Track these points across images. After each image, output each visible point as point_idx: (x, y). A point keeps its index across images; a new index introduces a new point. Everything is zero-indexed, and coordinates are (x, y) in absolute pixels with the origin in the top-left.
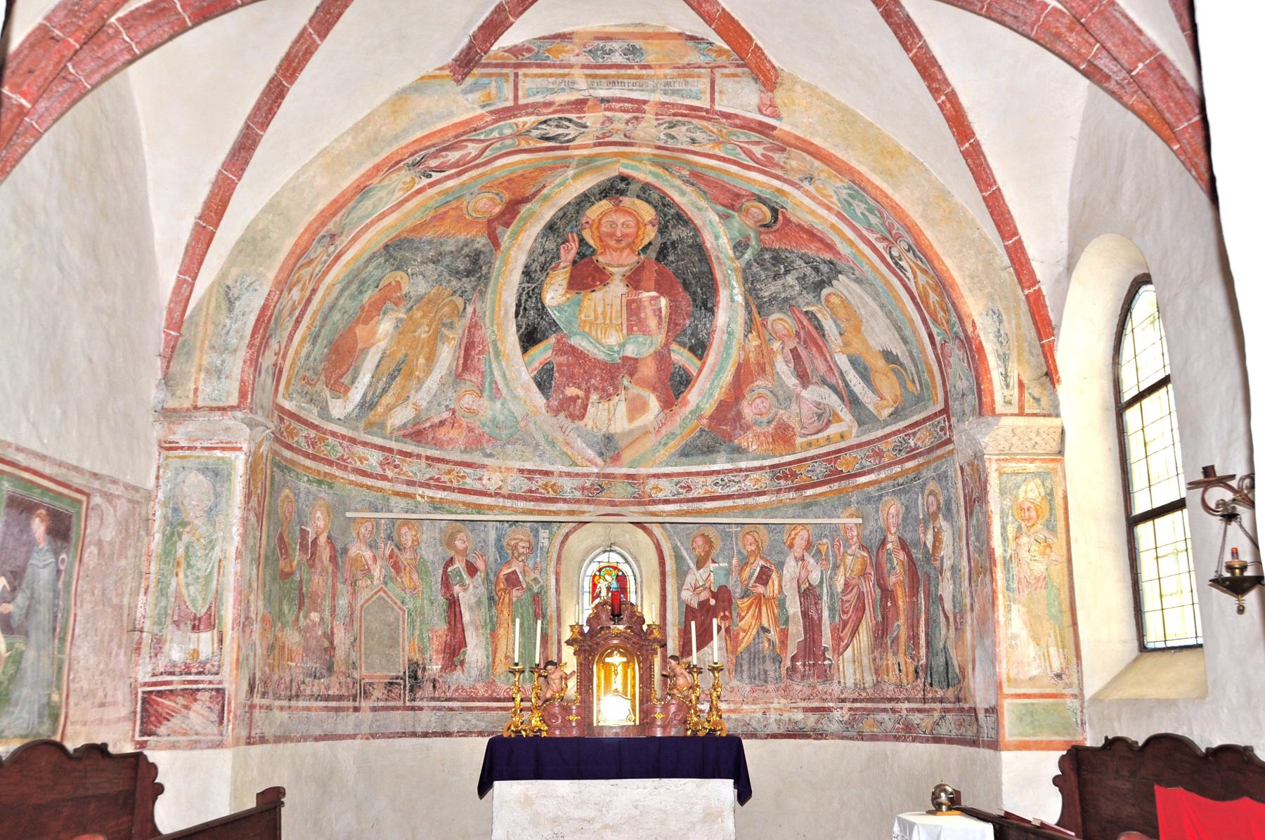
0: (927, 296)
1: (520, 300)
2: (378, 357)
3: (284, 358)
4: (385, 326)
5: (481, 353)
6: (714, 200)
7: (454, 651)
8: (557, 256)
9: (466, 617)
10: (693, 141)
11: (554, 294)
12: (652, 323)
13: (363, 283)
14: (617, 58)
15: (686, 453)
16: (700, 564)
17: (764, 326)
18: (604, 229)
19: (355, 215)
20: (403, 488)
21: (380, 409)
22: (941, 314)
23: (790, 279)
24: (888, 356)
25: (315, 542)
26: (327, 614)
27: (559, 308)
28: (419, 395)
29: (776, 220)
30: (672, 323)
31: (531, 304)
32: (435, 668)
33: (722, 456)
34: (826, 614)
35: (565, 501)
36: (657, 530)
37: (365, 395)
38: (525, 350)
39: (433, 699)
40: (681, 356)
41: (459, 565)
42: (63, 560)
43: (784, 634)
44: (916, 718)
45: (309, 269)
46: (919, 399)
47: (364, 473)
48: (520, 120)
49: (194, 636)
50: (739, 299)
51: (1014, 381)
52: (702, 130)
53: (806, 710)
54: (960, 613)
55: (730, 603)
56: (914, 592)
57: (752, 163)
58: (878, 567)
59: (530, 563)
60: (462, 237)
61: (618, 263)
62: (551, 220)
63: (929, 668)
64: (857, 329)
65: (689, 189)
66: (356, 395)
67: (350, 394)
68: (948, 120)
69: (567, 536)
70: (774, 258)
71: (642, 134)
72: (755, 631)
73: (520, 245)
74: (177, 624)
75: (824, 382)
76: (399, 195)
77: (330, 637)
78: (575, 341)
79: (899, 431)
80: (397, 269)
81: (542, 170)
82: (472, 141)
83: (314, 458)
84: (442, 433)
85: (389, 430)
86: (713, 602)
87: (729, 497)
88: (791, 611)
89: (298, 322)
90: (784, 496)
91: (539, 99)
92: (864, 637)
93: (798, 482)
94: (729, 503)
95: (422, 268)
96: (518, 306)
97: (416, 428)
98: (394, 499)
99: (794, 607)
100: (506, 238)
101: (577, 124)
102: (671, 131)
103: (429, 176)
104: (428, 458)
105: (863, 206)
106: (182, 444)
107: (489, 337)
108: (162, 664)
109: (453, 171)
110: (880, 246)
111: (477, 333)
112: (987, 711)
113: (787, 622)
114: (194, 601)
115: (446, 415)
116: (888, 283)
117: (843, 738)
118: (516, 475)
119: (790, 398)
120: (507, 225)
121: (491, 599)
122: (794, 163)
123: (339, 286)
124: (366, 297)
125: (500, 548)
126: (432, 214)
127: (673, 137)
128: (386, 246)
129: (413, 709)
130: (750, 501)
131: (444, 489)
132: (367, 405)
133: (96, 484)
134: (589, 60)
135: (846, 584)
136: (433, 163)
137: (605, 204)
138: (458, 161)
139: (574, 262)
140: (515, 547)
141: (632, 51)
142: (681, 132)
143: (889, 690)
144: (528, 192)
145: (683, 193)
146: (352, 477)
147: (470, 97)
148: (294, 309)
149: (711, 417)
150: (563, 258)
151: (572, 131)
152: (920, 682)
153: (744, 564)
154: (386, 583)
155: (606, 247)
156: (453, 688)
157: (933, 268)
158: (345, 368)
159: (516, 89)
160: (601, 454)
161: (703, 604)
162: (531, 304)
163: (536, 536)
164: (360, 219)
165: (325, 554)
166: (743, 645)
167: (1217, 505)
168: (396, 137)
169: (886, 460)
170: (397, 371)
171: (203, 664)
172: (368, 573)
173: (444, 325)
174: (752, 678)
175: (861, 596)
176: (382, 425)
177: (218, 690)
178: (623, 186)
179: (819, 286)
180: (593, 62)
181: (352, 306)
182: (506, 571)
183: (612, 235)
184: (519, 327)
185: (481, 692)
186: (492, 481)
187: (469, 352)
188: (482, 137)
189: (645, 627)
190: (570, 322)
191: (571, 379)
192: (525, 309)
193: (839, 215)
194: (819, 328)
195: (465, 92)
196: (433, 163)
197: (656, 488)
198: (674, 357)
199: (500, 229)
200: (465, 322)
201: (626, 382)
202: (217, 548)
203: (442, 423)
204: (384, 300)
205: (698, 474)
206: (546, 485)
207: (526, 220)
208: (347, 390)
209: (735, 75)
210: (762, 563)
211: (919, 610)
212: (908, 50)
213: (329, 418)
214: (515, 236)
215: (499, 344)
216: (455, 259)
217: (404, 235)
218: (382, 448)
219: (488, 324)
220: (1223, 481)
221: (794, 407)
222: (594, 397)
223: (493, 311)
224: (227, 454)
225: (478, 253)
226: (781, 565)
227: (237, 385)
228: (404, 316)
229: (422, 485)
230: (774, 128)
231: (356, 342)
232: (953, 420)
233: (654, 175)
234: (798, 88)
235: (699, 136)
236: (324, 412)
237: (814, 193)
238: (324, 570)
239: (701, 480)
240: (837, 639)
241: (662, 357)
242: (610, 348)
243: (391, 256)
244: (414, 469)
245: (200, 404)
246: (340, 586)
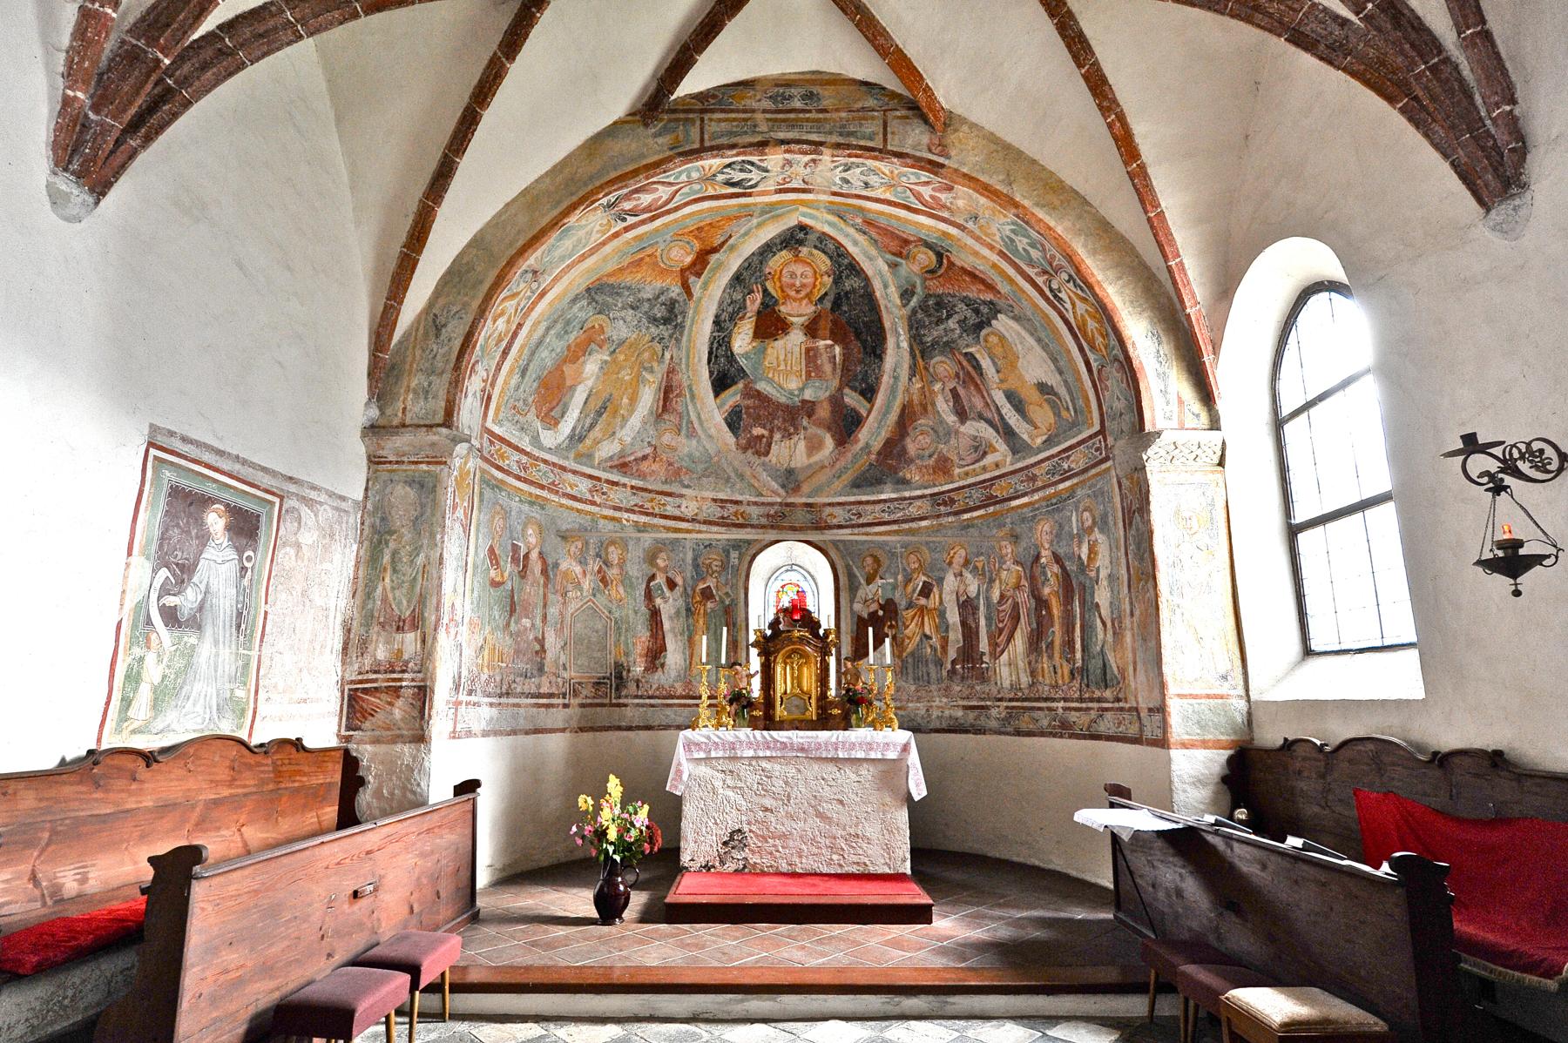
0: (1085, 324)
3: (493, 385)
4: (591, 367)
6: (884, 249)
7: (655, 655)
9: (667, 625)
10: (866, 184)
11: (742, 341)
12: (828, 368)
13: (568, 323)
14: (798, 104)
15: (858, 484)
16: (869, 581)
17: (926, 369)
19: (557, 254)
20: (610, 513)
21: (588, 442)
22: (1099, 340)
23: (952, 323)
24: (1043, 388)
25: (526, 556)
26: (538, 622)
27: (746, 356)
28: (624, 432)
29: (940, 263)
30: (845, 369)
32: (638, 669)
33: (888, 487)
34: (983, 622)
35: (752, 526)
36: (833, 554)
37: (574, 429)
38: (717, 395)
39: (636, 697)
40: (852, 399)
41: (660, 580)
42: (249, 559)
43: (945, 641)
44: (1073, 717)
45: (514, 302)
46: (1074, 425)
47: (574, 498)
48: (706, 163)
49: (399, 637)
50: (905, 345)
51: (1174, 399)
52: (874, 172)
54: (1117, 620)
55: (896, 613)
56: (1067, 600)
57: (921, 207)
58: (1032, 579)
59: (723, 580)
60: (658, 284)
61: (797, 312)
63: (1084, 671)
64: (1013, 366)
65: (860, 238)
66: (566, 427)
68: (1116, 139)
70: (937, 304)
71: (819, 180)
73: (711, 294)
74: (382, 625)
75: (981, 417)
76: (597, 238)
77: (541, 641)
78: (762, 386)
79: (1053, 456)
81: (730, 219)
82: (663, 183)
83: (526, 481)
84: (644, 466)
86: (881, 613)
87: (895, 522)
88: (951, 621)
89: (505, 353)
90: (944, 520)
91: (724, 141)
92: (1019, 643)
93: (956, 507)
94: (895, 527)
96: (710, 353)
98: (602, 522)
99: (953, 617)
100: (697, 285)
101: (759, 168)
102: (844, 175)
103: (624, 220)
105: (1025, 240)
106: (391, 458)
108: (367, 662)
110: (1040, 281)
112: (1150, 710)
113: (947, 630)
114: (400, 603)
115: (648, 450)
116: (1046, 316)
117: (1001, 733)
118: (709, 503)
119: (950, 433)
120: (699, 275)
121: (688, 610)
122: (960, 203)
123: (544, 325)
124: (572, 337)
125: (696, 566)
126: (629, 260)
127: (847, 182)
128: (588, 290)
129: (619, 705)
130: (914, 525)
131: (647, 514)
132: (576, 438)
133: (293, 488)
134: (767, 104)
135: (1002, 596)
136: (627, 205)
137: (785, 255)
139: (759, 312)
140: (710, 565)
141: (810, 96)
142: (855, 175)
143: (1045, 691)
144: (717, 242)
145: (856, 243)
146: (564, 501)
147: (660, 140)
148: (500, 340)
149: (879, 453)
151: (755, 176)
152: (1076, 684)
153: (908, 580)
157: (1095, 295)
159: (702, 133)
160: (783, 486)
161: (873, 615)
163: (728, 556)
164: (562, 259)
165: (536, 567)
166: (910, 649)
167: (1481, 475)
168: (591, 178)
169: (1040, 484)
170: (603, 409)
171: (406, 663)
172: (578, 586)
174: (917, 679)
175: (1016, 606)
176: (590, 456)
177: (419, 688)
178: (801, 235)
179: (980, 326)
180: (773, 107)
181: (560, 346)
184: (711, 373)
185: (680, 691)
186: (689, 508)
187: (668, 394)
188: (671, 180)
189: (821, 632)
190: (756, 369)
191: (757, 420)
193: (1001, 254)
194: (977, 367)
195: (655, 136)
196: (627, 205)
198: (847, 400)
199: (692, 279)
200: (665, 367)
201: (805, 422)
202: (422, 555)
203: (645, 458)
204: (590, 340)
205: (868, 502)
206: (736, 514)
208: (557, 423)
209: (907, 117)
210: (924, 578)
211: (1074, 617)
212: (1080, 66)
213: (541, 448)
214: (705, 286)
218: (591, 477)
220: (1484, 449)
221: (953, 441)
222: (777, 436)
224: (432, 468)
225: (673, 302)
226: (941, 581)
227: (443, 404)
229: (627, 511)
230: (943, 166)
232: (1110, 440)
233: (830, 224)
234: (965, 128)
235: (873, 180)
236: (536, 440)
237: (978, 232)
238: (536, 582)
239: (869, 508)
240: (993, 644)
241: (836, 401)
242: (791, 393)
244: (620, 496)
245: (408, 421)
246: (551, 597)
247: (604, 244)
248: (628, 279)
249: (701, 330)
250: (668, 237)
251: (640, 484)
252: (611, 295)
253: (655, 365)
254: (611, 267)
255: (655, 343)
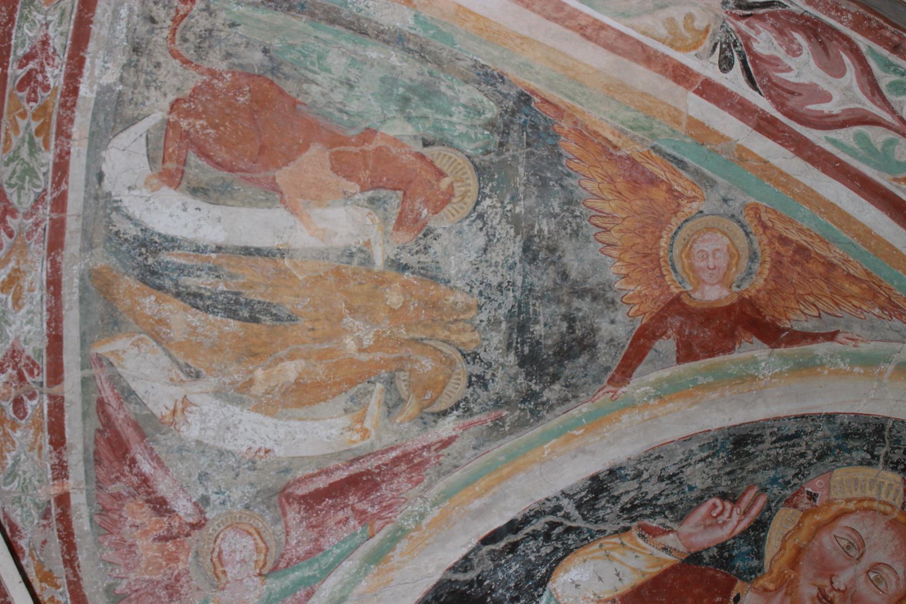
1: (526, 520)
2: (265, 241)
5: (361, 516)
8: (679, 512)
18: (826, 539)
21: (149, 302)
28: (210, 405)
31: (533, 550)
37: (172, 243)
60: (612, 271)
62: (761, 425)
67: (167, 192)
80: (480, 170)
84: (136, 515)
85: (104, 349)
95: (504, 230)
96: (513, 527)
97: (129, 433)
100: (659, 369)
103: (726, 64)
104: (63, 500)
107: (401, 517)
109: (762, 103)
111: (401, 483)
115: (183, 507)
120: (686, 353)
124: (399, 129)
128: (524, 99)
136: (765, 42)
138: (793, 91)
139: (695, 558)
150: (686, 529)
155: (786, 585)
158: (222, 155)
162: (533, 550)
170: (247, 310)
173: (391, 382)
176: (112, 323)
181: (365, 105)
183: (827, 571)
184: (465, 564)
187: (353, 487)
188: (885, 80)
192: (513, 547)
196: (765, 42)
199: (666, 345)
200: (416, 438)
203: (160, 506)
204: (404, 185)
207: (724, 380)
208: (173, 178)
215: (402, 546)
216: (550, 296)
217: (566, 125)
219: (432, 493)
223: (467, 484)
228: (379, 262)
231: (289, 159)
236: (115, 115)
243: (505, 133)
247: (649, 58)
248: (590, 184)
249: (555, 466)
250: (740, 199)
251: (82, 522)
252: (535, 170)
253: (411, 408)
254: (604, 118)
255: (463, 369)
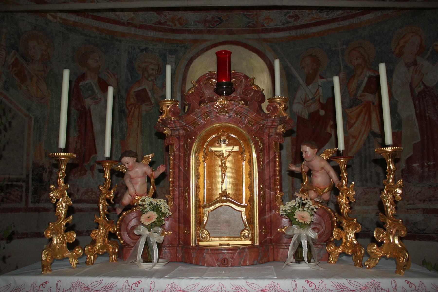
16: (309, 81)
35: (190, 32)
53: (426, 211)
69: (191, 61)
72: (365, 137)
86: (322, 113)
94: (334, 25)
129: (37, 210)
154: (7, 89)
156: (82, 190)
161: (314, 115)
182: (137, 89)
197: (268, 18)
